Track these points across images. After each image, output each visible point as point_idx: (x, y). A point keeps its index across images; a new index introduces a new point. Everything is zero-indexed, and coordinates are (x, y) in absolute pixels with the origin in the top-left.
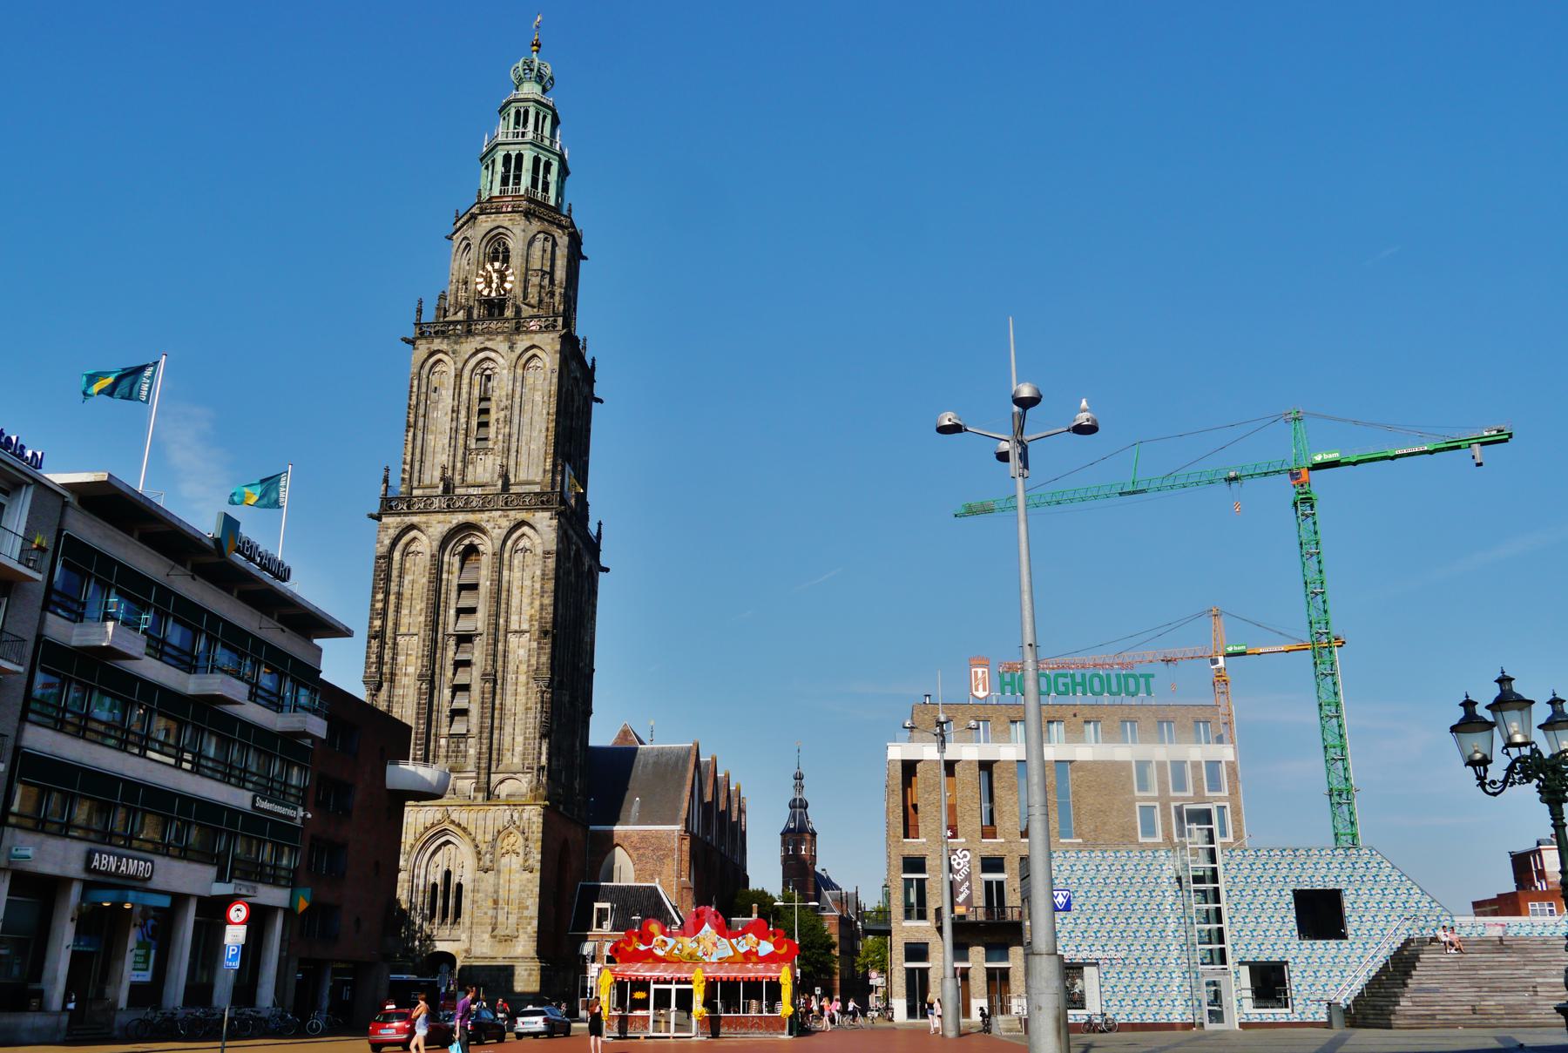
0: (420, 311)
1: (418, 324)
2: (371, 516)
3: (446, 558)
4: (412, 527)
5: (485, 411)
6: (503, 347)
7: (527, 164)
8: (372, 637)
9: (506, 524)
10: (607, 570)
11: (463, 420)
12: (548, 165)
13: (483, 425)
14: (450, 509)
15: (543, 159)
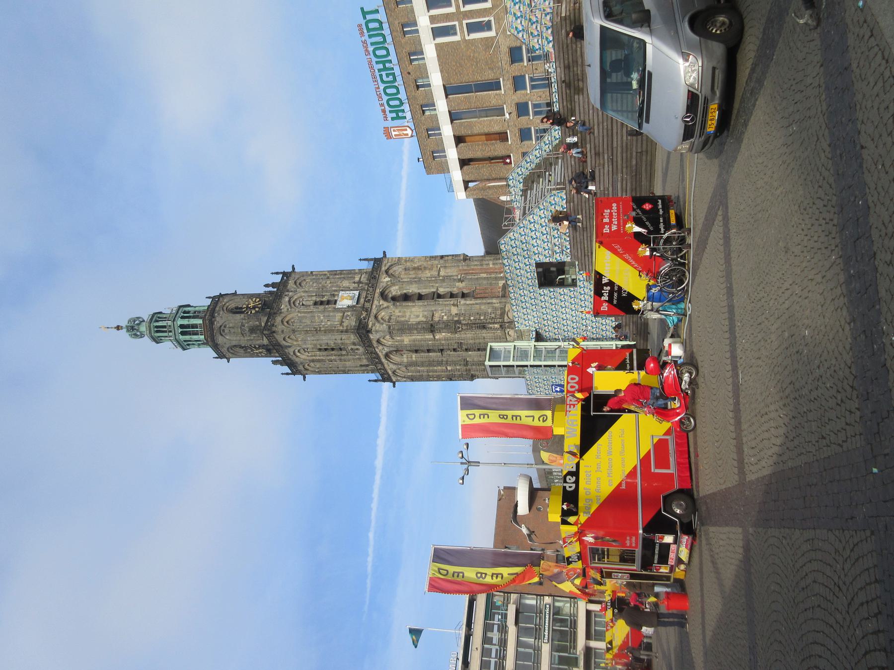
0: (287, 374)
1: (294, 373)
2: (394, 386)
3: (405, 360)
4: (394, 372)
5: (326, 349)
6: (291, 351)
7: (187, 337)
8: (451, 380)
9: (381, 347)
10: (384, 252)
11: (333, 358)
12: (182, 326)
13: (333, 349)
14: (382, 364)
15: (180, 330)
